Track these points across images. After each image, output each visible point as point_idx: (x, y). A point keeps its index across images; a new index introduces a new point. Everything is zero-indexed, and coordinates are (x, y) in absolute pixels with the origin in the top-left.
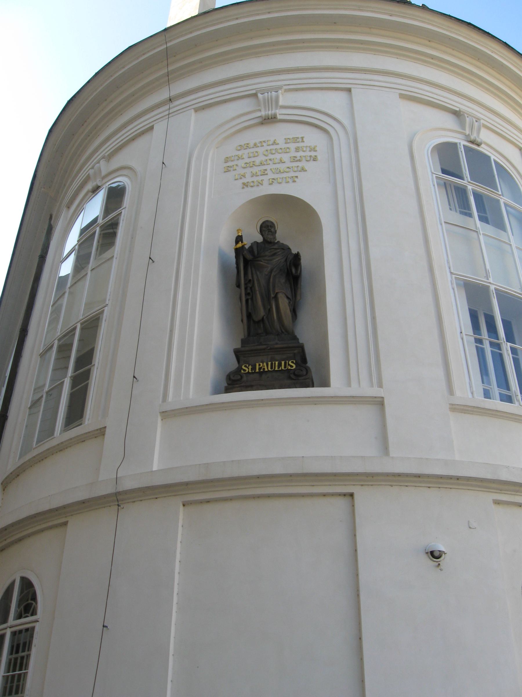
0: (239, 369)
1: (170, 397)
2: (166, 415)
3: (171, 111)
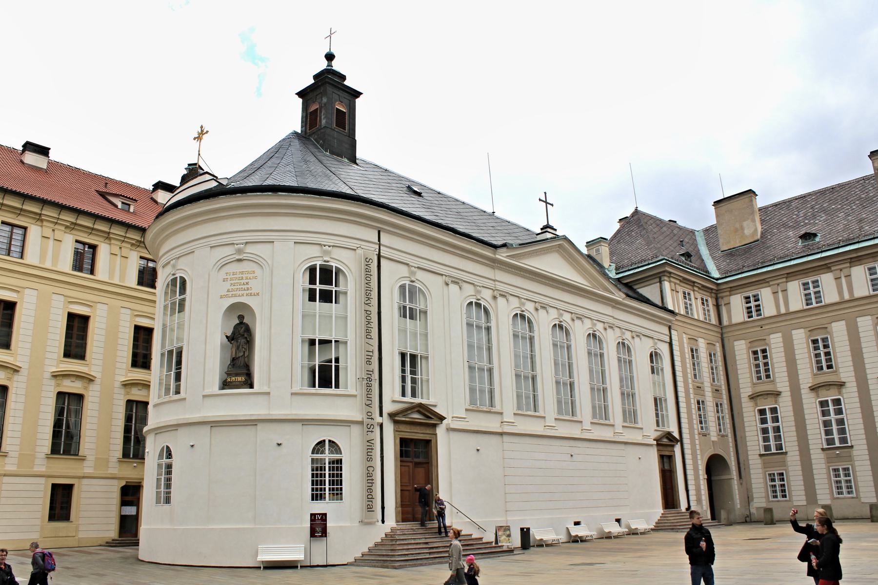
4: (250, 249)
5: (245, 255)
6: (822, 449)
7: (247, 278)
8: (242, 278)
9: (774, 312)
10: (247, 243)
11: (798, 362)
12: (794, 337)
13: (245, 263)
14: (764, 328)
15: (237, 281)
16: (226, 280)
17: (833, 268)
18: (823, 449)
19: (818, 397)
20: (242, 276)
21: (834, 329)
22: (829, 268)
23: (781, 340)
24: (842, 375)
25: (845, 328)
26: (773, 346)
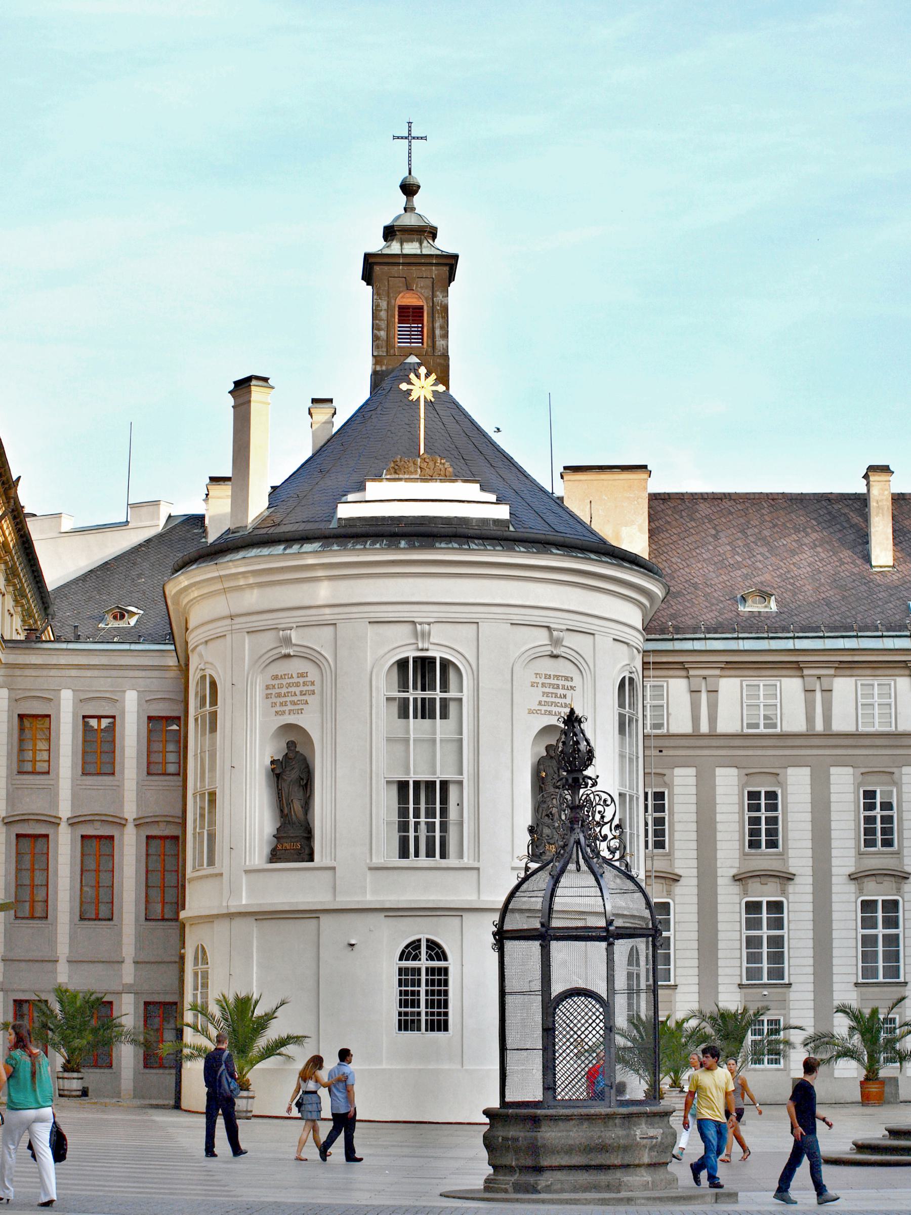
0: (277, 846)
1: (247, 863)
2: (246, 872)
3: (234, 627)
4: (571, 640)
5: (563, 649)
6: (739, 985)
7: (563, 687)
8: (558, 687)
9: (687, 729)
10: (568, 630)
11: (719, 827)
12: (718, 781)
13: (561, 659)
14: (664, 753)
15: (551, 690)
16: (535, 685)
17: (806, 672)
18: (740, 986)
19: (746, 893)
20: (556, 682)
21: (790, 780)
22: (801, 669)
23: (693, 781)
24: (791, 862)
25: (808, 780)
26: (677, 790)
